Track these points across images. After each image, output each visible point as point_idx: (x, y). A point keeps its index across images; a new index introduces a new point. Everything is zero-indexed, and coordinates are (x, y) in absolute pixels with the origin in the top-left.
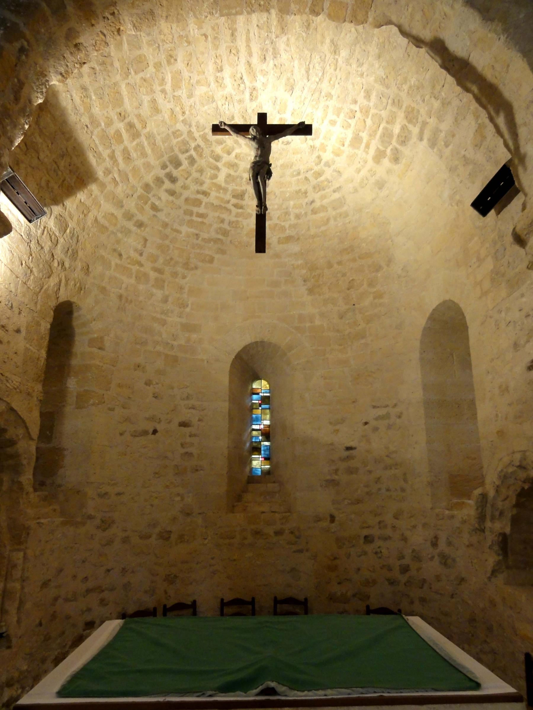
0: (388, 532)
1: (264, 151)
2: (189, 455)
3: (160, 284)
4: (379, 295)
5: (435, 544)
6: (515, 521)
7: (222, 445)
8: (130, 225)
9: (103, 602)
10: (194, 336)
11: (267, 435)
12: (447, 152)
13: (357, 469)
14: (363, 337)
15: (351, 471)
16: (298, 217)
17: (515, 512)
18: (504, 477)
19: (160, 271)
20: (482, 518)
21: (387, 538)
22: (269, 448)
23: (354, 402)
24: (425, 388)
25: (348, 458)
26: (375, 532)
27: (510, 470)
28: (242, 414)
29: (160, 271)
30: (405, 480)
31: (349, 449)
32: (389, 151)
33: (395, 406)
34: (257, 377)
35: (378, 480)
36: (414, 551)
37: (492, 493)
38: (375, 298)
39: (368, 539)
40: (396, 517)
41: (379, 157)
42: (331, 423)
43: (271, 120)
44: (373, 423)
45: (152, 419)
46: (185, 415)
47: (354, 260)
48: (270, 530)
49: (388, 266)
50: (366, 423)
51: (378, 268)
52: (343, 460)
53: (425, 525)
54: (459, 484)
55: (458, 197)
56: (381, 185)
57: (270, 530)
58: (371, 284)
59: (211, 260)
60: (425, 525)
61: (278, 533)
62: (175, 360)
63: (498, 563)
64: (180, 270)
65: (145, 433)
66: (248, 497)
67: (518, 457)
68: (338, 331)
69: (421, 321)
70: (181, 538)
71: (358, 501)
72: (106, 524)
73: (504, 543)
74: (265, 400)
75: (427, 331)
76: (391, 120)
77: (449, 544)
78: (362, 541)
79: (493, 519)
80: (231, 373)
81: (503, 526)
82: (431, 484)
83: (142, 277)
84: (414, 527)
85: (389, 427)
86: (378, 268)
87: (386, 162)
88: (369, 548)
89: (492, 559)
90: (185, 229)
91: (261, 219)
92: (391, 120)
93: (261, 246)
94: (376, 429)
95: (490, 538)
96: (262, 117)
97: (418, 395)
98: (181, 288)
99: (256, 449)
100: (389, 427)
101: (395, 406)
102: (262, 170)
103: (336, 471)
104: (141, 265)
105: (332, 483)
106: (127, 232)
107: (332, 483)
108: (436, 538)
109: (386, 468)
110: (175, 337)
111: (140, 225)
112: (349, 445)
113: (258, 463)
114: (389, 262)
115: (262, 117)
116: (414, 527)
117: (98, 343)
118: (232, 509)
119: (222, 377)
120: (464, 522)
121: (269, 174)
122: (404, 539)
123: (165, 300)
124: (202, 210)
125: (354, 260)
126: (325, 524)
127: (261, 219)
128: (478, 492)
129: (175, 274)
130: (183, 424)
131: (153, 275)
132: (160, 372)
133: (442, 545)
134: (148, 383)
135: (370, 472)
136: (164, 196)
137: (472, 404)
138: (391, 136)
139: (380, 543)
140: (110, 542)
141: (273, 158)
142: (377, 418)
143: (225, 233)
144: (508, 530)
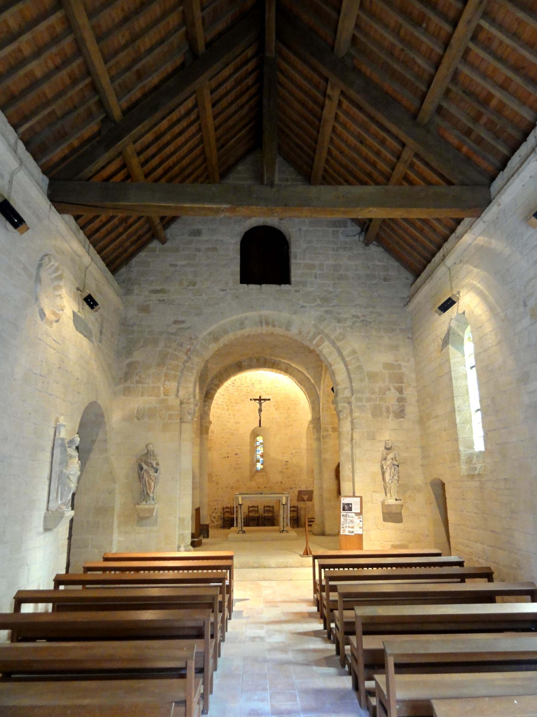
1: (260, 404)
2: (237, 464)
3: (228, 410)
4: (297, 413)
7: (248, 460)
8: (221, 396)
9: (218, 504)
10: (238, 425)
11: (262, 456)
15: (287, 469)
16: (271, 388)
19: (228, 406)
22: (263, 461)
24: (307, 445)
25: (286, 465)
26: (292, 486)
28: (254, 449)
29: (228, 406)
31: (287, 462)
34: (258, 436)
35: (295, 471)
39: (291, 488)
43: (262, 398)
45: (227, 453)
46: (237, 451)
48: (262, 487)
51: (296, 405)
57: (262, 487)
58: (294, 410)
59: (244, 400)
61: (265, 487)
62: (232, 434)
64: (234, 405)
65: (225, 458)
66: (256, 477)
70: (237, 488)
71: (289, 477)
72: (217, 484)
74: (261, 444)
80: (250, 437)
82: (307, 472)
83: (223, 409)
86: (296, 405)
88: (291, 491)
90: (236, 393)
91: (260, 421)
94: (294, 456)
96: (260, 397)
98: (234, 410)
99: (258, 461)
102: (260, 410)
103: (283, 469)
104: (222, 405)
105: (281, 472)
106: (220, 398)
107: (281, 472)
110: (233, 426)
111: (223, 395)
113: (259, 466)
115: (260, 397)
117: (213, 432)
118: (251, 480)
119: (248, 439)
123: (229, 415)
124: (241, 388)
126: (279, 484)
127: (260, 421)
129: (232, 406)
130: (236, 454)
131: (226, 407)
132: (229, 438)
134: (226, 442)
136: (231, 387)
140: (218, 489)
142: (296, 452)
143: (248, 393)
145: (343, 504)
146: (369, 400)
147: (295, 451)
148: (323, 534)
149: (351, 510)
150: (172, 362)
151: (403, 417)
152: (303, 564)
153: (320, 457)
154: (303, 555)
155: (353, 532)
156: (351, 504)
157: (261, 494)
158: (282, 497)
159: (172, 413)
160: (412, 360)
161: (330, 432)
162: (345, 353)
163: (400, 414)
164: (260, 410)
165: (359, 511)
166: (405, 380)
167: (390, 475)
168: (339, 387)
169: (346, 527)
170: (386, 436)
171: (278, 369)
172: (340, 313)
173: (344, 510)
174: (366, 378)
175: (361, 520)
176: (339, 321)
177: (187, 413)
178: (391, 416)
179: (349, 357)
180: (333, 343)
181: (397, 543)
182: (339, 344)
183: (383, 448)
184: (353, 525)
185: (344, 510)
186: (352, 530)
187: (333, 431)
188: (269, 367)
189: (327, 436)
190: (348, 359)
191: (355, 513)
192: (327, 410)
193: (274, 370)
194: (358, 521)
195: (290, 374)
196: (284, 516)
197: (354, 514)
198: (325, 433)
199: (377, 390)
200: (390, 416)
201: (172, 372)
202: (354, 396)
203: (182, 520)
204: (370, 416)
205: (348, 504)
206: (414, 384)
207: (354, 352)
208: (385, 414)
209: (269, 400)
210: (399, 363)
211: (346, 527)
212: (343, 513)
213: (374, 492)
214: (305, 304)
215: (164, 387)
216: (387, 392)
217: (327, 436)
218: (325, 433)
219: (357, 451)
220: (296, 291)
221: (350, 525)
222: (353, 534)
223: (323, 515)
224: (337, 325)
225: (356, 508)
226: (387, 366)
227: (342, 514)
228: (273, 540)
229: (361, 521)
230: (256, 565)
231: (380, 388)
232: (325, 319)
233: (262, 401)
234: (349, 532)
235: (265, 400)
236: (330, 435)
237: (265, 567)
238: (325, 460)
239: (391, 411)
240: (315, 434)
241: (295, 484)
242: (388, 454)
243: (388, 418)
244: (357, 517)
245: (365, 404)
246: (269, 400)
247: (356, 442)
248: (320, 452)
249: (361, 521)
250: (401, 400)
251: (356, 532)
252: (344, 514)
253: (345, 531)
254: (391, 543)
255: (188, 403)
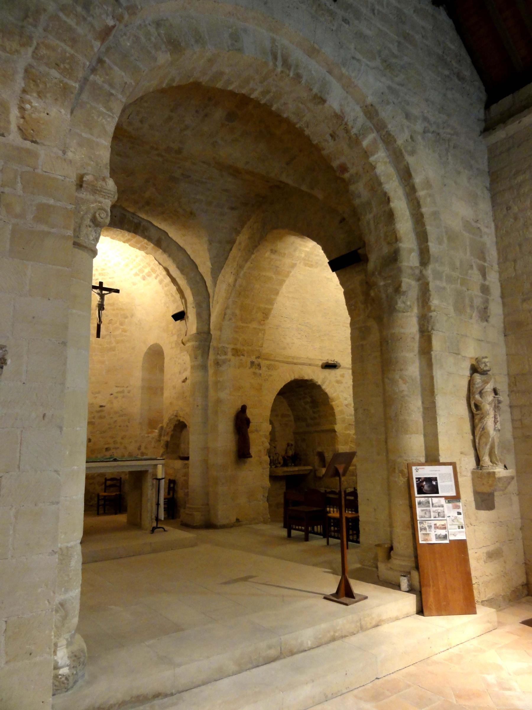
0: (117, 446)
4: (124, 331)
5: (139, 449)
6: (172, 436)
12: (166, 289)
13: (105, 417)
14: (114, 351)
15: (101, 417)
17: (172, 432)
18: (170, 420)
20: (160, 435)
21: (116, 448)
23: (106, 383)
24: (143, 380)
26: (112, 446)
27: (172, 417)
30: (129, 422)
31: (101, 406)
32: (141, 275)
33: (127, 387)
36: (129, 453)
37: (165, 426)
38: (122, 331)
40: (122, 438)
41: (136, 275)
42: (93, 393)
44: (115, 395)
47: (114, 310)
49: (131, 317)
50: (112, 394)
51: (126, 317)
52: (98, 412)
53: (136, 441)
54: (152, 424)
55: (167, 305)
56: (134, 284)
60: (136, 441)
63: (164, 452)
67: (175, 412)
68: (101, 345)
69: (145, 349)
71: (104, 432)
73: (167, 445)
75: (147, 354)
76: (145, 267)
77: (146, 448)
78: (104, 450)
79: (164, 436)
81: (167, 438)
84: (131, 442)
85: (123, 397)
86: (126, 317)
87: (139, 278)
89: (162, 451)
92: (145, 267)
93: (98, 335)
94: (116, 397)
95: (162, 443)
96: (101, 283)
97: (139, 383)
100: (123, 397)
101: (127, 387)
102: (101, 307)
103: (94, 418)
108: (140, 446)
109: (119, 416)
112: (101, 405)
114: (132, 316)
115: (101, 283)
116: (131, 442)
120: (153, 438)
121: (103, 309)
122: (125, 448)
125: (114, 310)
128: (160, 425)
133: (143, 449)
135: (112, 418)
137: (162, 389)
138: (143, 272)
139: (114, 451)
141: (105, 302)
142: (117, 393)
144: (169, 440)
145: (419, 478)
146: (450, 279)
147: (115, 390)
148: (209, 525)
149: (437, 492)
150: (53, 41)
151: (487, 321)
152: (363, 623)
153: (206, 396)
154: (337, 594)
155: (445, 537)
156: (435, 479)
157: (115, 460)
158: (156, 465)
159: (52, 202)
160: (493, 225)
161: (229, 356)
162: (418, 180)
163: (484, 315)
164: (101, 307)
165: (453, 493)
166: (488, 259)
167: (495, 422)
168: (400, 245)
169: (430, 527)
170: (471, 351)
171: (145, 237)
172: (408, 104)
173: (420, 491)
174: (445, 240)
175: (461, 511)
176: (408, 116)
177: (88, 222)
178: (475, 314)
179: (423, 189)
180: (397, 157)
181: (492, 548)
182: (410, 160)
183: (468, 373)
184: (443, 523)
185: (420, 491)
186: (443, 532)
187: (233, 355)
188: (129, 231)
189: (224, 362)
190: (421, 193)
191: (446, 498)
192: (230, 319)
193: (139, 238)
194: (454, 513)
195: (165, 251)
196: (152, 500)
197: (443, 501)
198: (223, 357)
199: (458, 264)
200: (474, 315)
201: (54, 73)
202: (430, 267)
203: (64, 555)
204: (451, 309)
205: (429, 480)
206: (496, 267)
207: (428, 184)
208: (468, 310)
209: (117, 291)
210: (479, 225)
211: (430, 527)
212: (419, 498)
213: (462, 453)
214: (359, 56)
215: (22, 109)
216: (470, 271)
217: (224, 362)
218: (223, 357)
219: (438, 374)
220: (345, 20)
221: (439, 523)
222: (447, 542)
223: (207, 494)
224: (405, 122)
225: (446, 487)
226: (467, 225)
227: (417, 500)
228: (154, 551)
229: (459, 513)
230: (273, 652)
231: (461, 262)
232: (388, 103)
233: (104, 292)
234: (438, 537)
235: (110, 290)
236: (230, 361)
237: (292, 653)
238: (219, 401)
239: (475, 307)
240: (200, 358)
241: (115, 442)
242: (486, 382)
243: (471, 318)
244: (450, 505)
245: (444, 284)
246: (117, 291)
247: (436, 356)
248: (203, 388)
249: (459, 513)
250: (485, 290)
251: (452, 538)
252: (422, 500)
253: (429, 535)
254: (485, 550)
255: (95, 191)
